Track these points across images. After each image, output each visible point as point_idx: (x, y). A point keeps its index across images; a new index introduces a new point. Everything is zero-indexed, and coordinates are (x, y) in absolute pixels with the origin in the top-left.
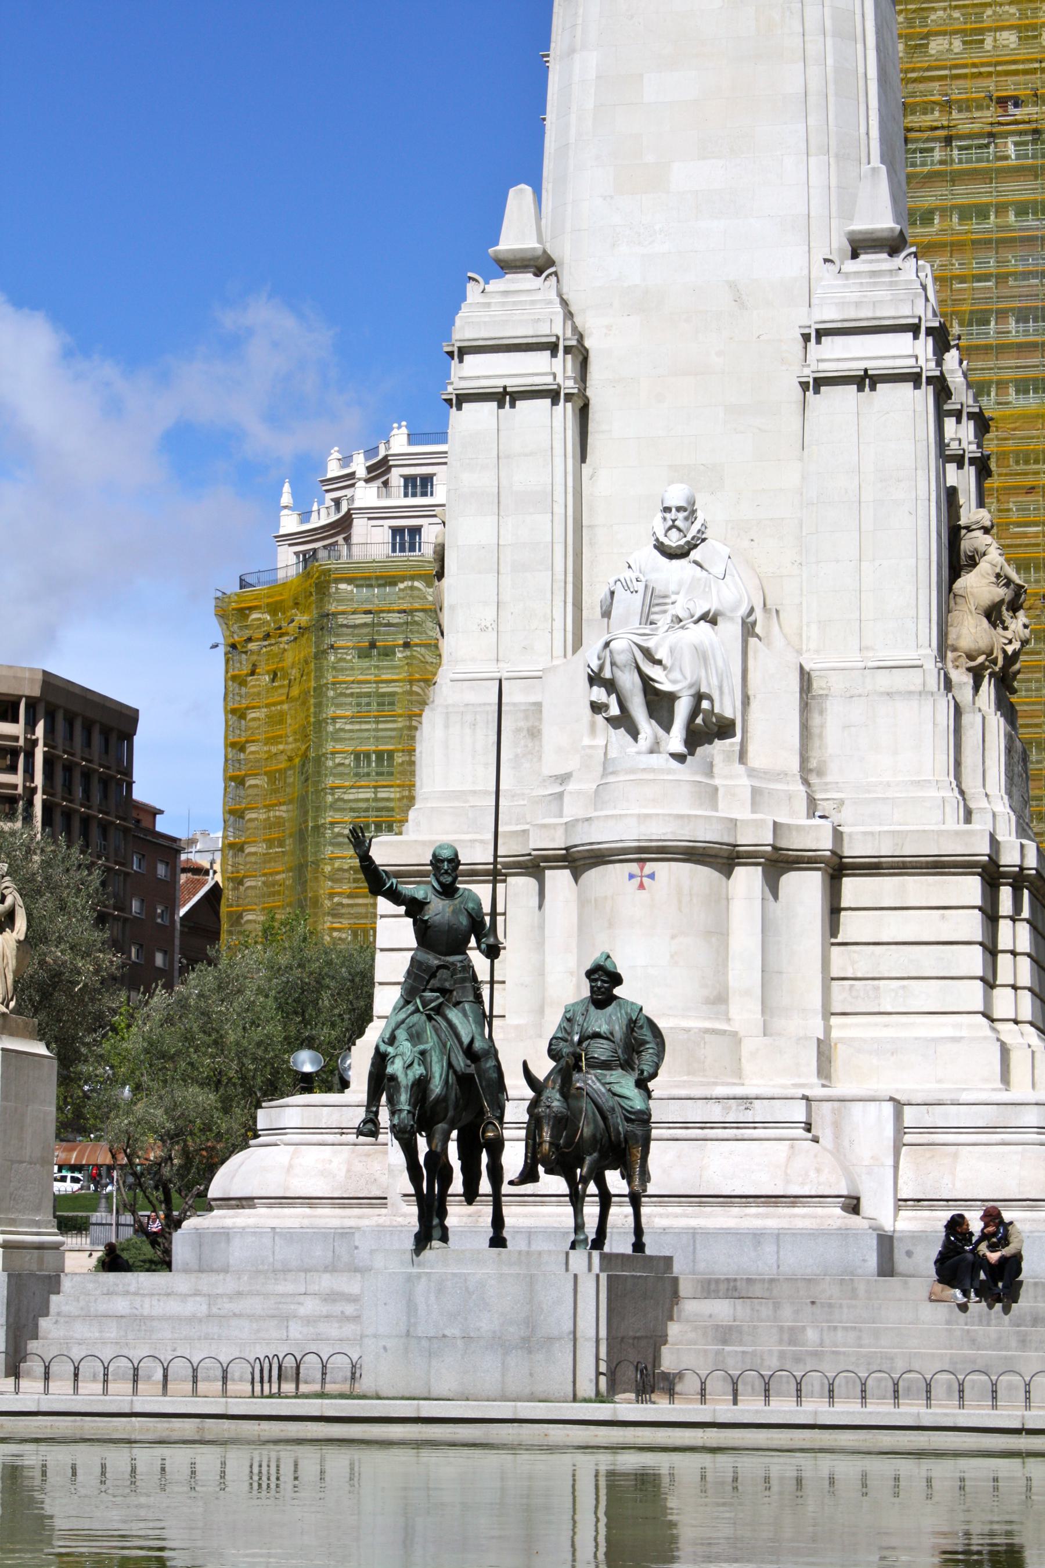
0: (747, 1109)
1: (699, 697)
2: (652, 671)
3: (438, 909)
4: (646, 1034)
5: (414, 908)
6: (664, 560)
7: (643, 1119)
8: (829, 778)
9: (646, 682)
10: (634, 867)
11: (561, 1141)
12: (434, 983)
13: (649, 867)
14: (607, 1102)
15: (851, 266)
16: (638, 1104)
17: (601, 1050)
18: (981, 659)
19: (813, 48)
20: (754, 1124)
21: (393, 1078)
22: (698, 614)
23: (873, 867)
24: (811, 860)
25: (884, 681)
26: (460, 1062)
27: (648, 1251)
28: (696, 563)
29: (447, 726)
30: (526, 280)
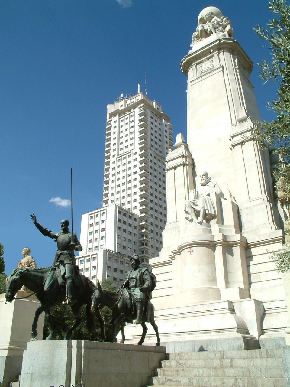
0: (213, 306)
1: (205, 210)
2: (195, 207)
10: (188, 249)
11: (99, 307)
13: (192, 249)
22: (206, 195)
24: (236, 244)
27: (161, 345)
28: (208, 186)
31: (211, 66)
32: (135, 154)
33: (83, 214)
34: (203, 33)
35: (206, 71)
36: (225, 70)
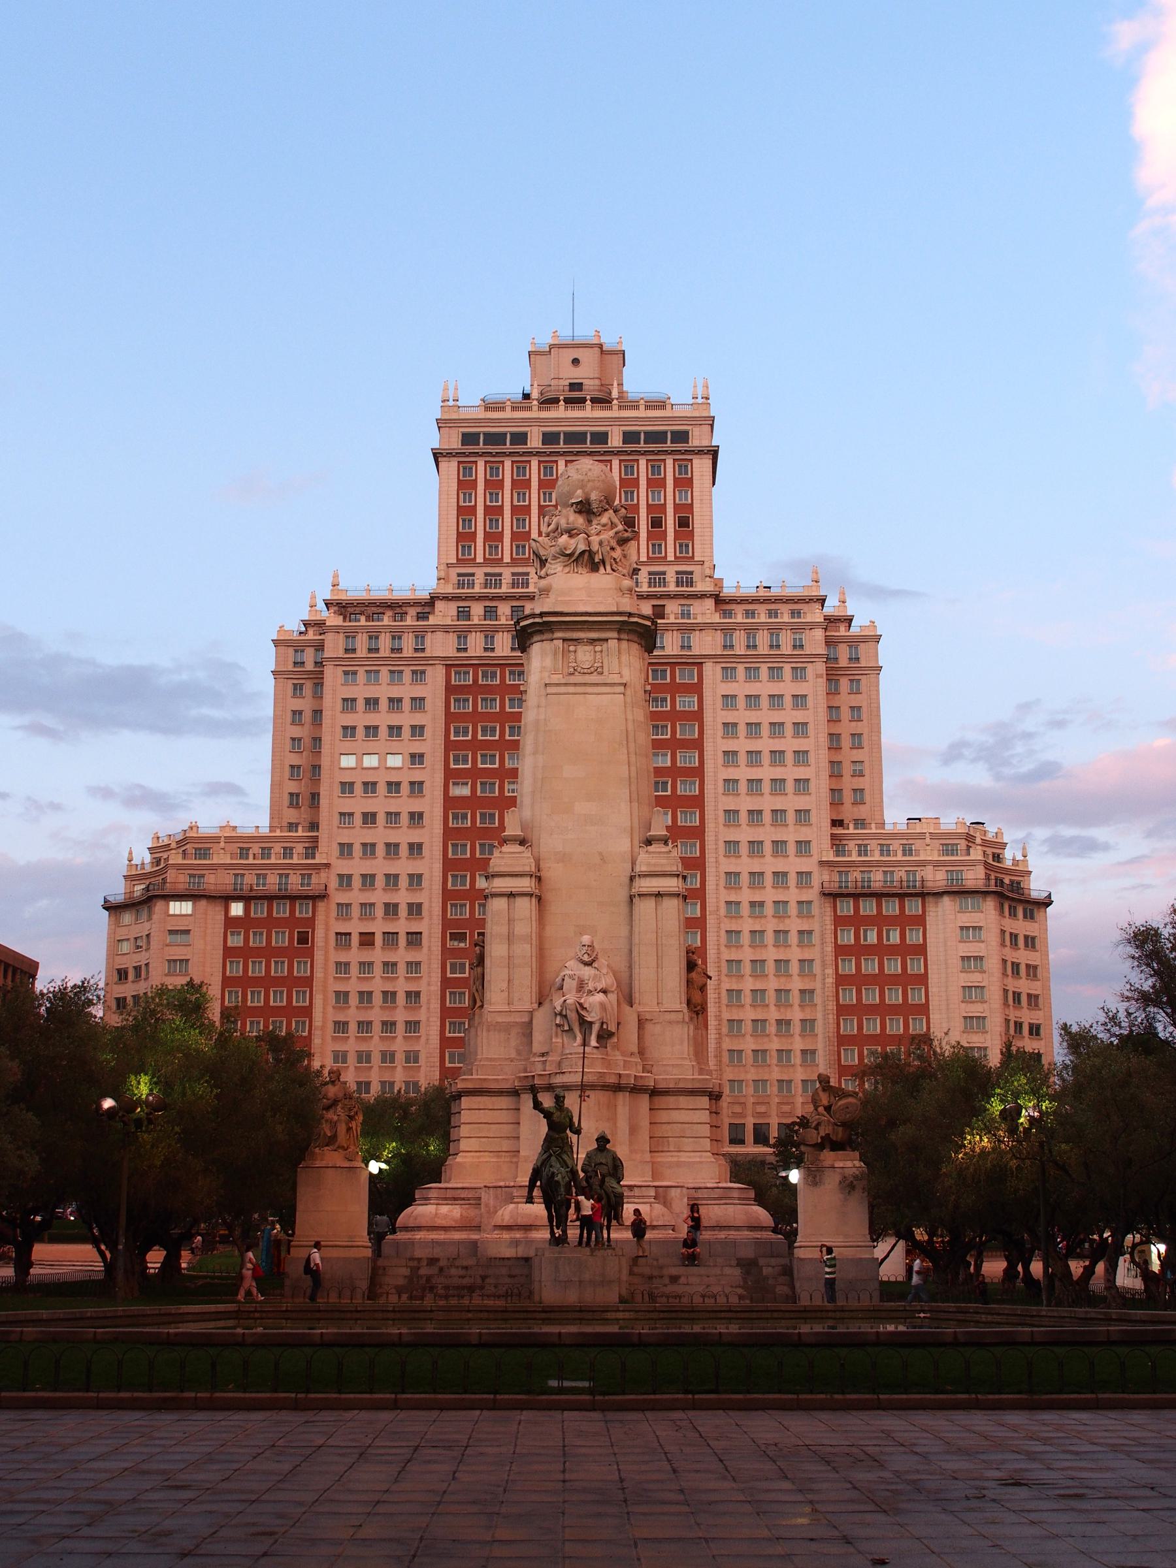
3: (557, 1116)
5: (547, 1115)
6: (582, 966)
7: (621, 1196)
9: (581, 1017)
16: (619, 1190)
18: (699, 1008)
19: (633, 759)
20: (634, 1197)
21: (558, 1182)
23: (666, 1092)
25: (668, 1017)
29: (488, 1031)
30: (517, 848)
34: (587, 554)
35: (586, 671)
36: (628, 692)
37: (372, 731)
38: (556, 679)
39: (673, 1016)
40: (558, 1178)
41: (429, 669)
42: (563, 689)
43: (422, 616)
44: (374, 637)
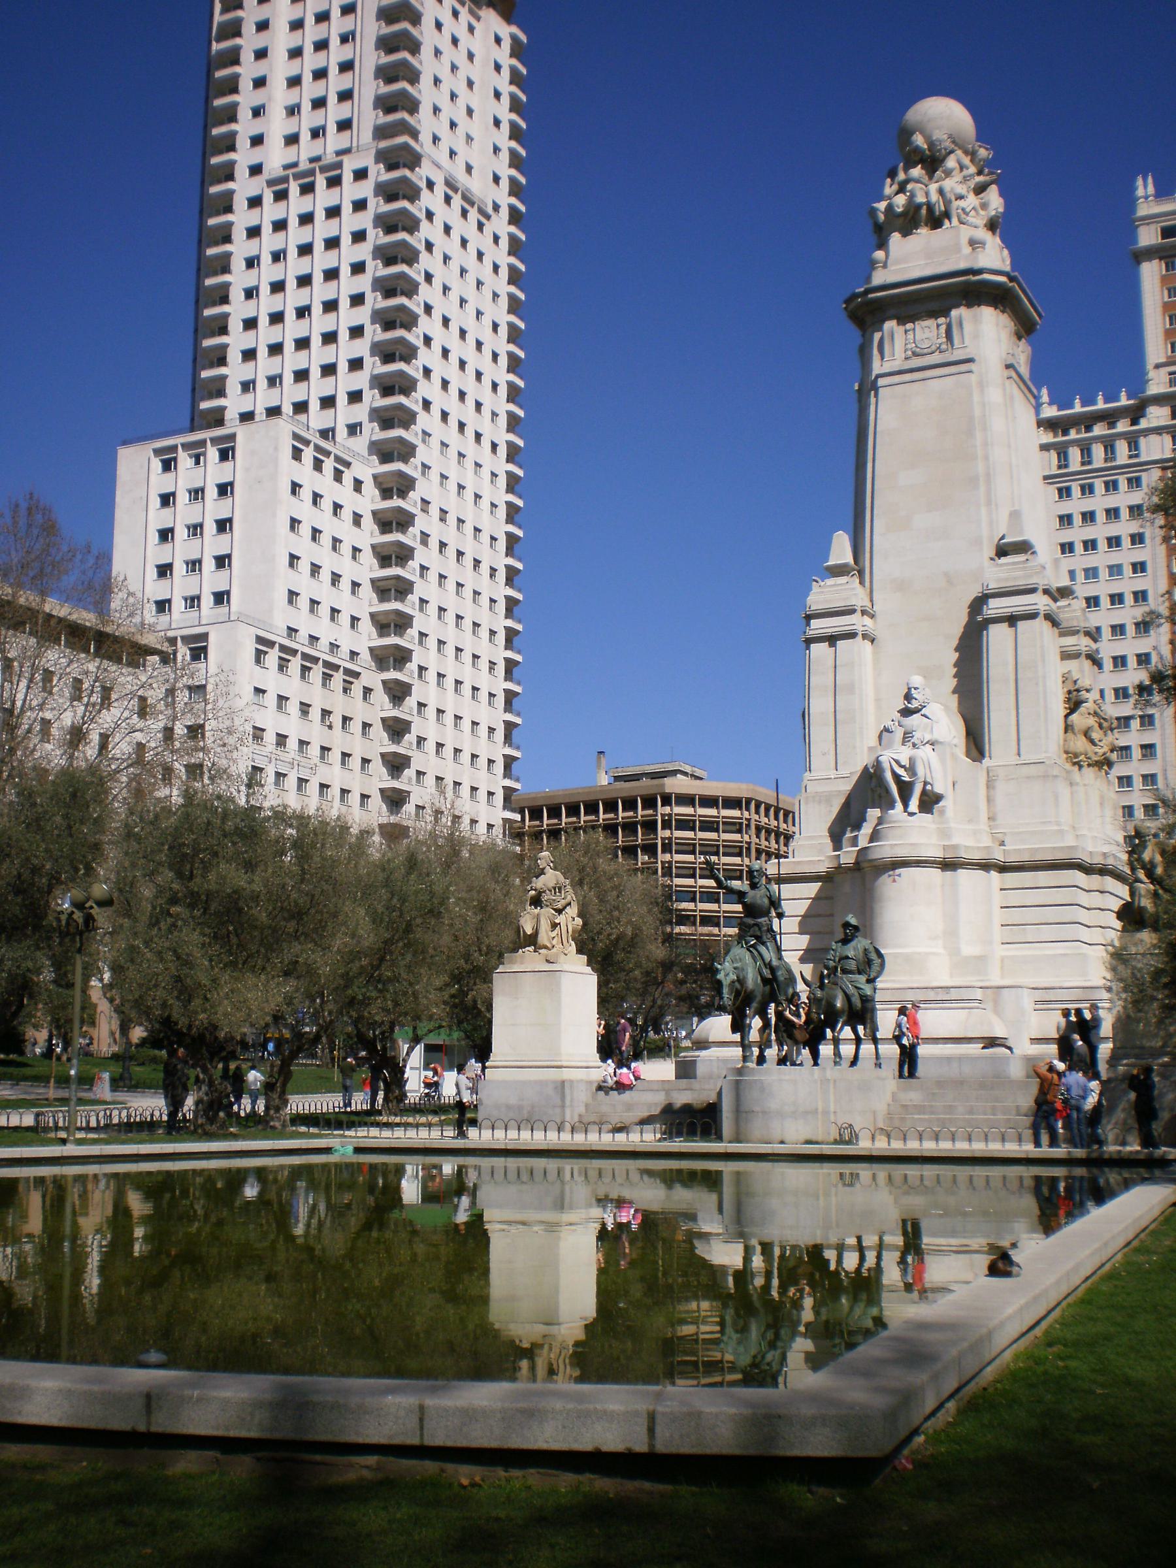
1: (926, 783)
4: (873, 956)
8: (998, 822)
9: (896, 777)
12: (751, 932)
13: (898, 871)
14: (851, 990)
15: (1004, 560)
16: (867, 989)
17: (852, 965)
21: (719, 983)
25: (1025, 770)
26: (766, 973)
29: (807, 803)
31: (940, 341)
32: (360, 175)
33: (126, 443)
34: (924, 211)
37: (1090, 545)
38: (887, 367)
39: (1032, 770)
40: (720, 976)
41: (1144, 475)
42: (896, 379)
43: (1134, 422)
44: (1086, 451)
